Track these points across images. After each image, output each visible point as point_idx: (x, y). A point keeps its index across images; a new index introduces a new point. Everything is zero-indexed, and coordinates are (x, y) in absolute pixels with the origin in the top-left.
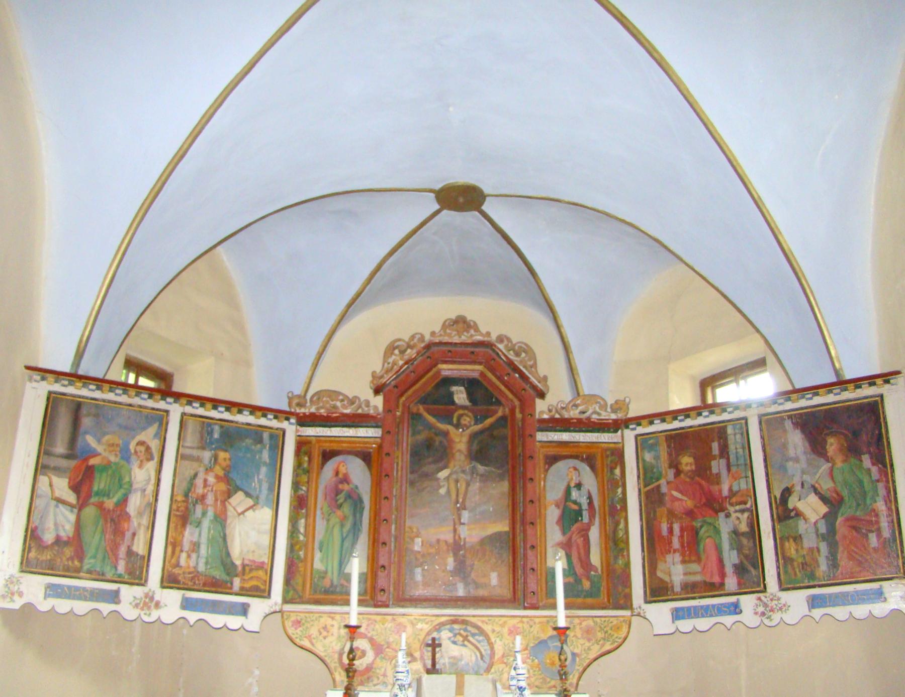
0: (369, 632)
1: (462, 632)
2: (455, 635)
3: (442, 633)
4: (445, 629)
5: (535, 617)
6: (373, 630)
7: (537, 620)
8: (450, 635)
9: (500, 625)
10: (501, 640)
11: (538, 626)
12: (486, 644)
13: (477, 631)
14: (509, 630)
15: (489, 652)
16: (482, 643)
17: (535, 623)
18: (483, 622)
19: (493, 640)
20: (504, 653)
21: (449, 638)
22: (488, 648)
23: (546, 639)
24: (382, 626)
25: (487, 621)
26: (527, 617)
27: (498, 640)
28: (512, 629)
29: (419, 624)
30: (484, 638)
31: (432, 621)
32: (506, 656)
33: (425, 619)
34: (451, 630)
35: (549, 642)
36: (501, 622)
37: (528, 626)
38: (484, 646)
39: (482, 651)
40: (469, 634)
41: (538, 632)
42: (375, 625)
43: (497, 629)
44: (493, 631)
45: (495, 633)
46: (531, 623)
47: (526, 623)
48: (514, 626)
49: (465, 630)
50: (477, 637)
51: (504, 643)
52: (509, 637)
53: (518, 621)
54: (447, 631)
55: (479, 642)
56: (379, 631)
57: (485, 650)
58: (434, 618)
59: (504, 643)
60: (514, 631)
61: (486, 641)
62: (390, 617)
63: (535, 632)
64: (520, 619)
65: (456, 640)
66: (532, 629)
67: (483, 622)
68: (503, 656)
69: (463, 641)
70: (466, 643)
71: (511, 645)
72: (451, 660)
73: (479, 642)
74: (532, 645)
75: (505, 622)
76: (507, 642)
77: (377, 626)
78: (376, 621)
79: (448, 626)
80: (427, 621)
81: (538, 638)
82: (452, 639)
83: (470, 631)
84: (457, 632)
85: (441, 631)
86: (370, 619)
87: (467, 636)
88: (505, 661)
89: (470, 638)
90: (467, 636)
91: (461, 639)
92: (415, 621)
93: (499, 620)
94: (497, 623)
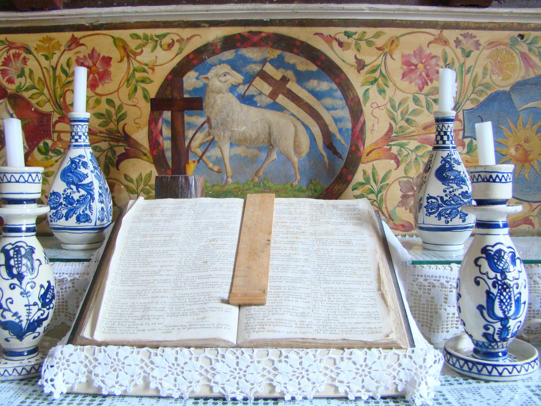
0: (10, 81)
1: (269, 69)
2: (249, 80)
3: (210, 74)
4: (221, 62)
5: (479, 27)
6: (21, 74)
7: (484, 36)
8: (239, 78)
9: (379, 49)
10: (381, 91)
11: (487, 52)
12: (341, 103)
13: (314, 68)
14: (407, 63)
15: (349, 125)
16: (328, 101)
17: (477, 44)
18: (329, 39)
19: (360, 92)
20: (391, 129)
21: (233, 88)
22: (345, 113)
23: (508, 89)
24: (45, 63)
25: (343, 38)
26: (456, 26)
27: (373, 90)
28: (414, 61)
29: (147, 50)
30: (334, 86)
31: (180, 41)
32: (397, 137)
33: (164, 36)
34: (235, 66)
35: (515, 98)
36: (379, 42)
37: (459, 51)
38: (334, 109)
39: (327, 117)
40: (290, 74)
41: (485, 68)
42: (25, 60)
43: (368, 58)
44: (361, 65)
45: (363, 72)
46: (468, 44)
47: (453, 45)
48: (419, 53)
49: (279, 63)
50: (313, 83)
51: (391, 100)
52: (404, 84)
53: (432, 38)
54: (226, 68)
55: (318, 95)
56: (38, 74)
57: (336, 120)
58: (186, 33)
59: (391, 100)
60: (420, 66)
61: (339, 94)
62: (66, 37)
63: (479, 70)
64: (436, 32)
65: (252, 91)
66: (469, 62)
67: (329, 39)
68: (388, 136)
69: (273, 95)
70: (281, 99)
71: (412, 106)
72: (239, 150)
73: (318, 95)
74: (469, 106)
75: (393, 42)
76: (399, 97)
77: (32, 64)
78: (28, 51)
79: (229, 55)
80: (167, 41)
81: (487, 86)
82: (241, 89)
83: (292, 67)
84: (257, 68)
85: (209, 70)
86: (11, 45)
87: (285, 80)
88: (395, 150)
89: (293, 86)
90: (285, 80)
91: (267, 89)
92: (133, 44)
93: (377, 36)
94: (370, 43)
